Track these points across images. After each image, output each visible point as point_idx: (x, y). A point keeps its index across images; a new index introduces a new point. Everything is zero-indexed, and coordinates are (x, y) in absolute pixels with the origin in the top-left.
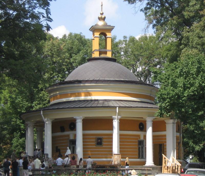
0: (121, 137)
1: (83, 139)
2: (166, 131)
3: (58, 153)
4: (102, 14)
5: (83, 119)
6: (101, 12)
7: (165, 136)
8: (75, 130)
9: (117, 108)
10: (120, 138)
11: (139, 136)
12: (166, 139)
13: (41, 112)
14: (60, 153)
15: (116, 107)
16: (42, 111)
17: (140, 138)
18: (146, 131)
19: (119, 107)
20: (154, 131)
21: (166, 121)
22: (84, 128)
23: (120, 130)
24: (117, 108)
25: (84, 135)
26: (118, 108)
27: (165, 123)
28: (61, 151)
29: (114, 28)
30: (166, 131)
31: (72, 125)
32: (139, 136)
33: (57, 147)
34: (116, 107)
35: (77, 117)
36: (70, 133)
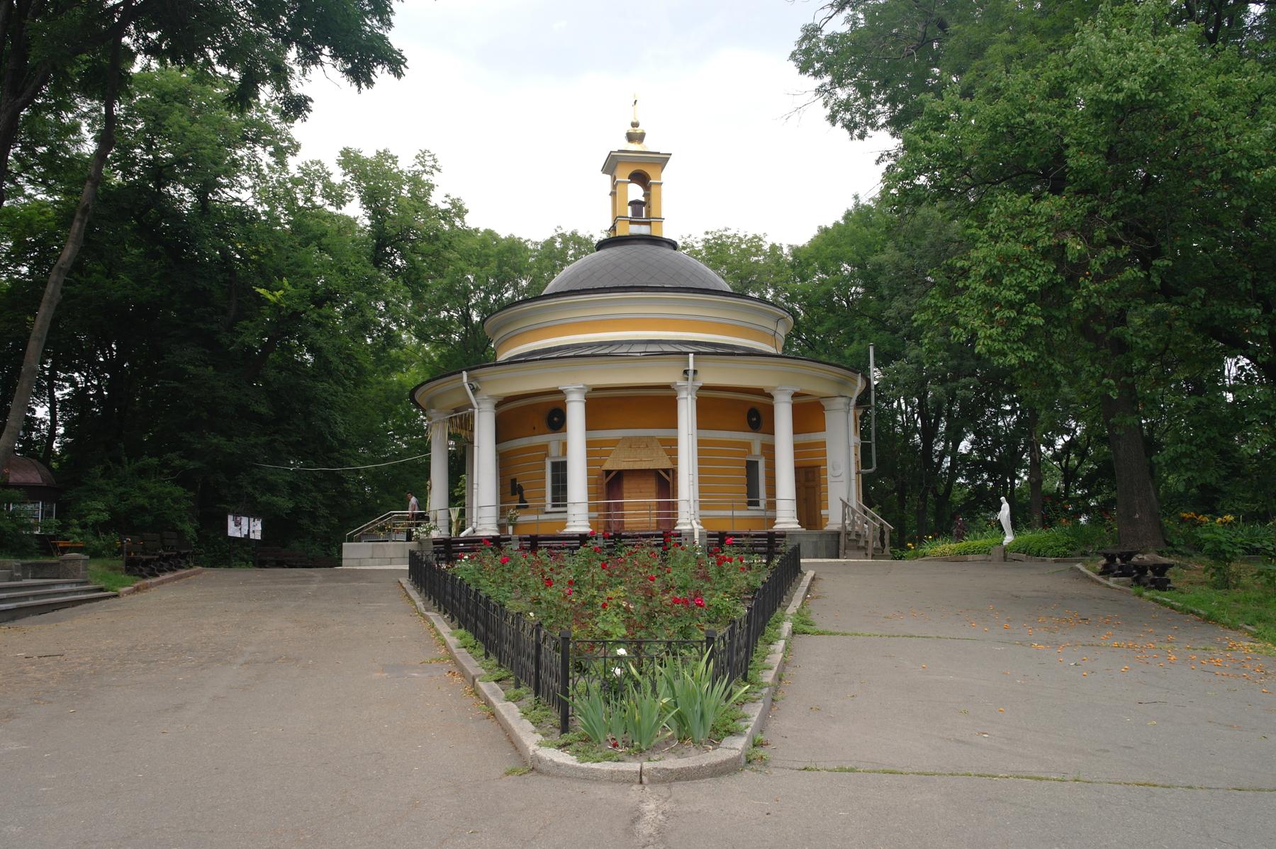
0: (703, 446)
1: (589, 454)
2: (825, 430)
3: (518, 496)
4: (635, 125)
5: (586, 391)
6: (635, 121)
7: (823, 444)
8: (566, 431)
9: (691, 355)
10: (700, 452)
11: (747, 445)
12: (824, 454)
13: (462, 378)
14: (522, 500)
15: (687, 353)
16: (464, 373)
17: (750, 452)
18: (771, 431)
19: (695, 354)
20: (798, 428)
21: (824, 403)
22: (590, 425)
23: (699, 428)
24: (691, 355)
25: (589, 444)
26: (694, 358)
27: (823, 408)
28: (524, 492)
29: (668, 159)
30: (825, 430)
31: (556, 419)
32: (747, 445)
33: (514, 481)
34: (687, 353)
35: (571, 388)
36: (550, 439)
